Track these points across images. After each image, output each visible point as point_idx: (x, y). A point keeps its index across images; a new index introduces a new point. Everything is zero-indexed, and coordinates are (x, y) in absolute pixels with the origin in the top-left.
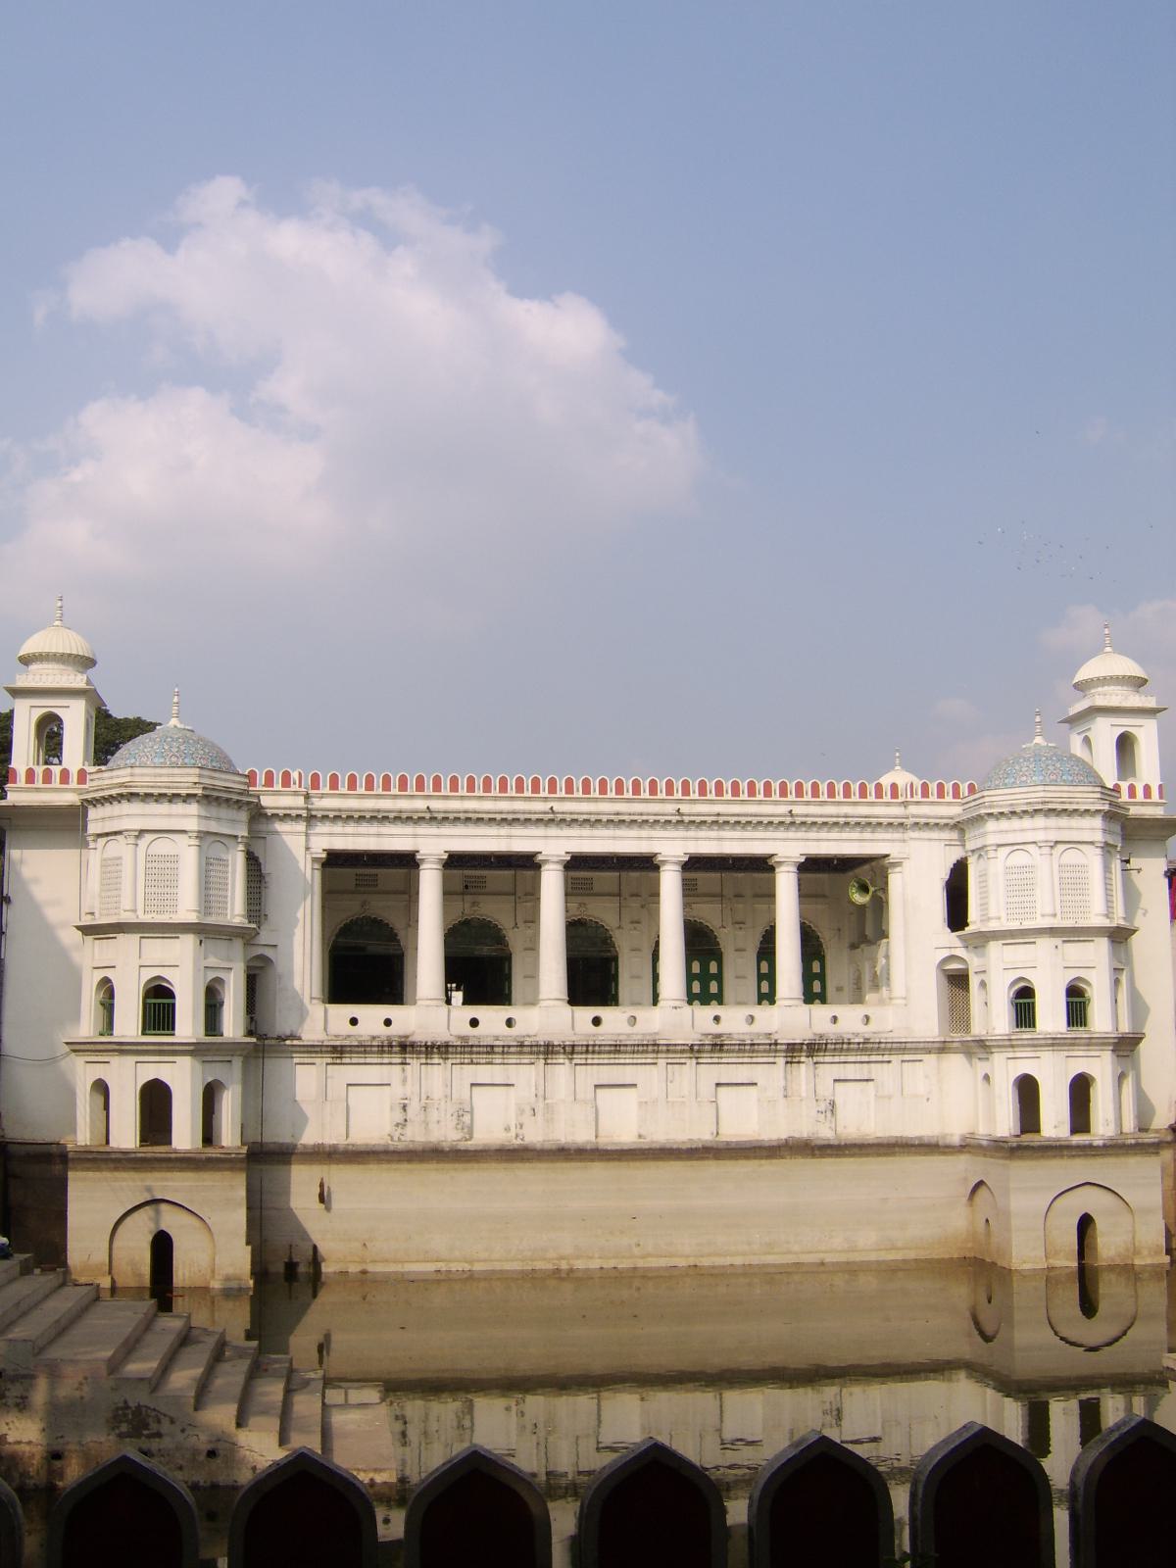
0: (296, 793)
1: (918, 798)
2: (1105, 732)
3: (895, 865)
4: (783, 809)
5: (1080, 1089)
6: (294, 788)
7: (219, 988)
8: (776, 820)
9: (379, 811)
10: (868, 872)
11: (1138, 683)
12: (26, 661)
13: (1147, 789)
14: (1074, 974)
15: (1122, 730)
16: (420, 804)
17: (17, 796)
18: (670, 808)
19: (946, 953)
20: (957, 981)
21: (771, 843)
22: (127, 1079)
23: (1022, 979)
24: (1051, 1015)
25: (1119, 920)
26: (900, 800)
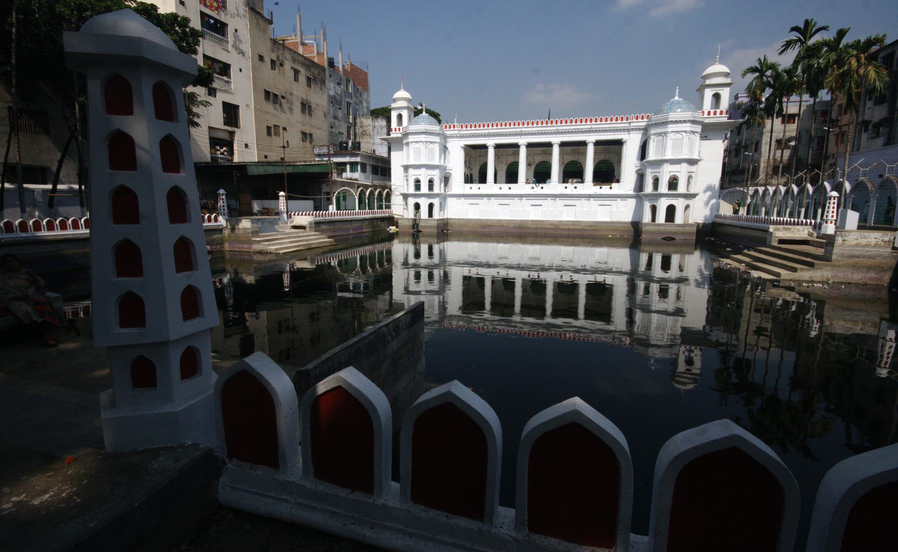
0: (456, 130)
1: (634, 120)
2: (709, 94)
3: (626, 142)
4: (590, 127)
5: (671, 210)
6: (456, 128)
7: (432, 180)
8: (587, 130)
9: (477, 133)
10: (619, 143)
11: (727, 75)
12: (395, 101)
13: (721, 113)
14: (672, 174)
15: (715, 92)
16: (487, 131)
17: (392, 135)
18: (555, 128)
19: (638, 168)
20: (641, 177)
21: (623, 135)
22: (412, 201)
23: (656, 176)
24: (663, 188)
25: (696, 157)
26: (629, 121)
